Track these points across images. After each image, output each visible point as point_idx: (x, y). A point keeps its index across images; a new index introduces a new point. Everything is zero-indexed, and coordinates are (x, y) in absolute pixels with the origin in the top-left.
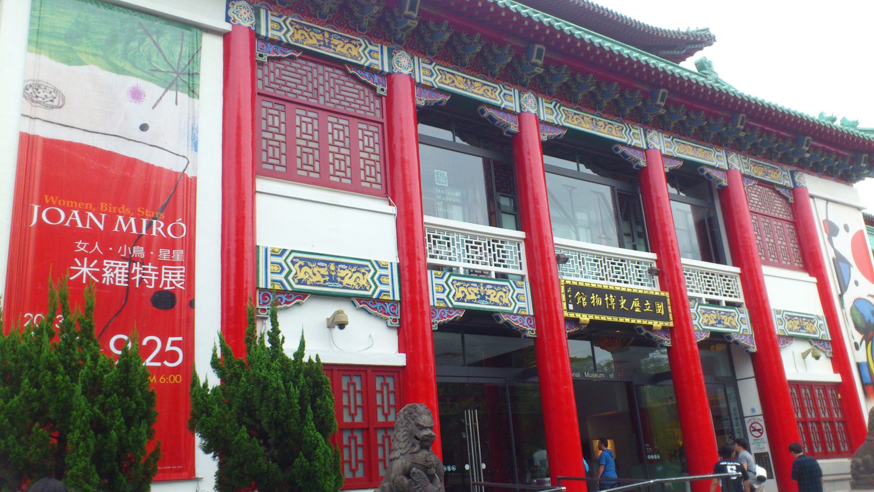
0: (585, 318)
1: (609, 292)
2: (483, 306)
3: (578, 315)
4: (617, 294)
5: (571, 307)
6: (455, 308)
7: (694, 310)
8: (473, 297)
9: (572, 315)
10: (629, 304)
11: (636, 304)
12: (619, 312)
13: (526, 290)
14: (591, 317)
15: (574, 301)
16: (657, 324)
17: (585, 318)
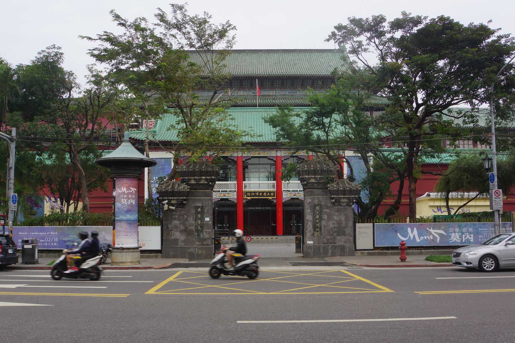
0: (249, 198)
1: (257, 192)
2: (224, 197)
3: (247, 198)
4: (259, 192)
5: (246, 196)
6: (218, 198)
7: (284, 194)
8: (222, 196)
9: (246, 198)
10: (259, 194)
11: (261, 194)
12: (259, 196)
13: (235, 193)
14: (251, 198)
15: (247, 195)
16: (270, 198)
17: (249, 198)
